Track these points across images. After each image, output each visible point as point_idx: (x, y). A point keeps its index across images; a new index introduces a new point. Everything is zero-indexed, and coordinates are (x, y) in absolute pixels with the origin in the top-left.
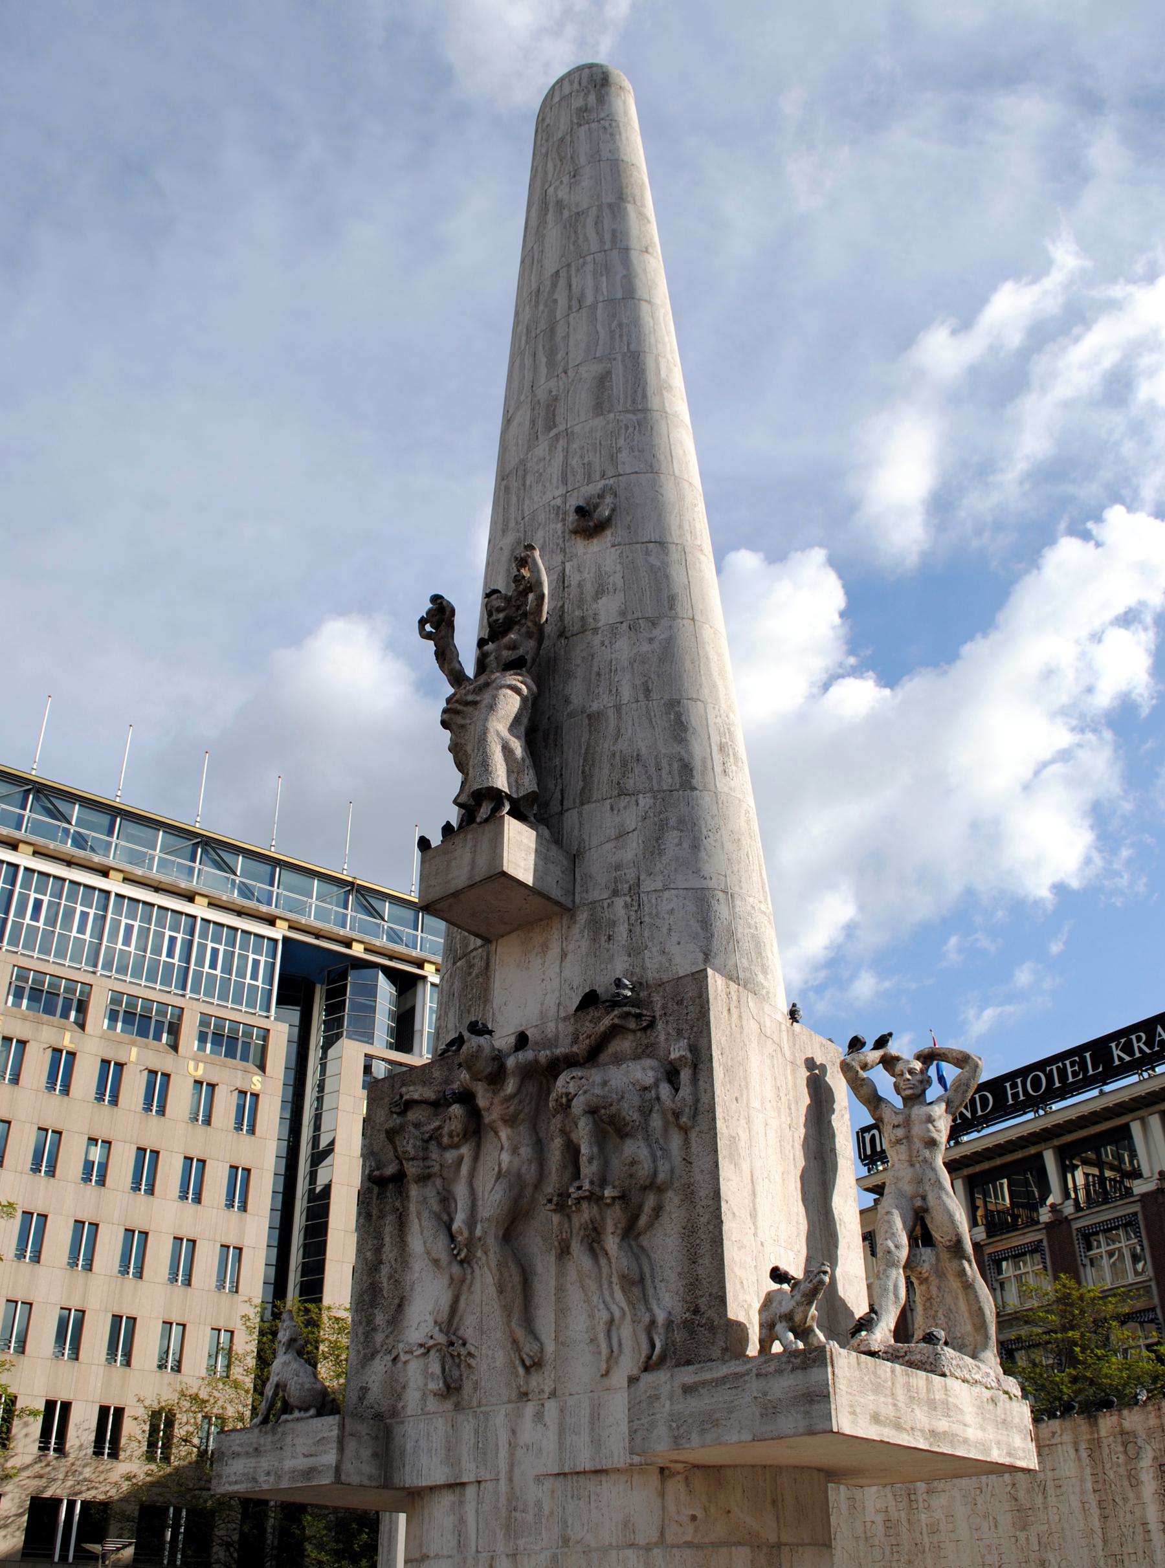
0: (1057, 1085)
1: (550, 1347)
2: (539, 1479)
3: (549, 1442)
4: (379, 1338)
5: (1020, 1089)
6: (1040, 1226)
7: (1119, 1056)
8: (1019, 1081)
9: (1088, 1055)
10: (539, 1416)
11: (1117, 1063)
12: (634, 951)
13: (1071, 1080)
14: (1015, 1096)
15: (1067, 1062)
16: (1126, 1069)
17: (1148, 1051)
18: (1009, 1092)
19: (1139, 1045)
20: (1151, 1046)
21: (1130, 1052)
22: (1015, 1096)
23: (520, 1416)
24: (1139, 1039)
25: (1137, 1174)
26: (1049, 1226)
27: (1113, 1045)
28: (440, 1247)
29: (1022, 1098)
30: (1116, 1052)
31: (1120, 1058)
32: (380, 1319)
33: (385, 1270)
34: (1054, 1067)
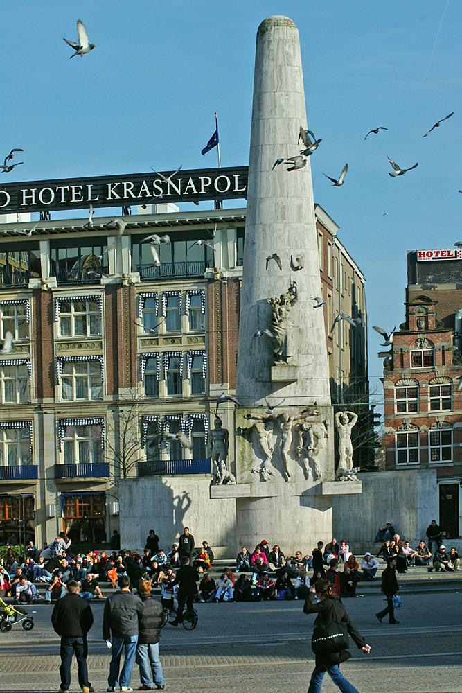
0: (63, 201)
3: (294, 491)
4: (246, 467)
5: (33, 197)
6: (29, 291)
7: (112, 193)
8: (33, 190)
9: (89, 187)
10: (291, 486)
11: (110, 198)
13: (73, 200)
14: (29, 200)
15: (73, 188)
16: (114, 203)
17: (133, 196)
18: (24, 197)
19: (128, 191)
20: (136, 193)
21: (121, 194)
22: (29, 200)
23: (286, 485)
24: (129, 186)
25: (105, 270)
27: (109, 185)
29: (34, 203)
30: (110, 191)
31: (113, 195)
32: (246, 463)
34: (63, 188)
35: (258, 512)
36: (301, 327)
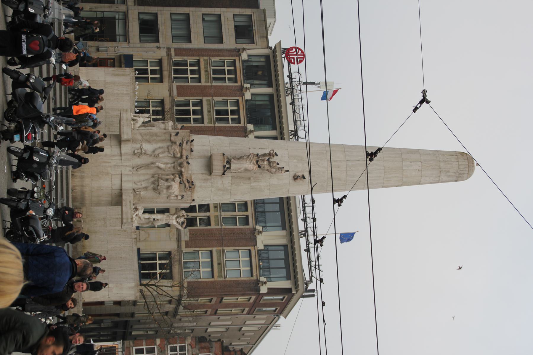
1: (139, 173)
2: (121, 171)
3: (126, 173)
4: (145, 137)
10: (130, 171)
12: (201, 187)
26: (245, 128)
28: (157, 152)
32: (148, 137)
33: (155, 138)
35: (110, 146)
36: (252, 179)
